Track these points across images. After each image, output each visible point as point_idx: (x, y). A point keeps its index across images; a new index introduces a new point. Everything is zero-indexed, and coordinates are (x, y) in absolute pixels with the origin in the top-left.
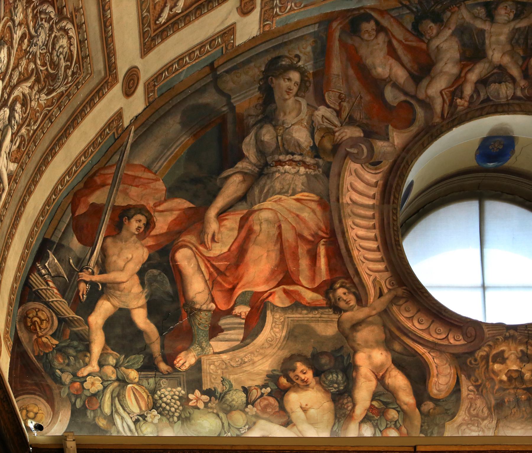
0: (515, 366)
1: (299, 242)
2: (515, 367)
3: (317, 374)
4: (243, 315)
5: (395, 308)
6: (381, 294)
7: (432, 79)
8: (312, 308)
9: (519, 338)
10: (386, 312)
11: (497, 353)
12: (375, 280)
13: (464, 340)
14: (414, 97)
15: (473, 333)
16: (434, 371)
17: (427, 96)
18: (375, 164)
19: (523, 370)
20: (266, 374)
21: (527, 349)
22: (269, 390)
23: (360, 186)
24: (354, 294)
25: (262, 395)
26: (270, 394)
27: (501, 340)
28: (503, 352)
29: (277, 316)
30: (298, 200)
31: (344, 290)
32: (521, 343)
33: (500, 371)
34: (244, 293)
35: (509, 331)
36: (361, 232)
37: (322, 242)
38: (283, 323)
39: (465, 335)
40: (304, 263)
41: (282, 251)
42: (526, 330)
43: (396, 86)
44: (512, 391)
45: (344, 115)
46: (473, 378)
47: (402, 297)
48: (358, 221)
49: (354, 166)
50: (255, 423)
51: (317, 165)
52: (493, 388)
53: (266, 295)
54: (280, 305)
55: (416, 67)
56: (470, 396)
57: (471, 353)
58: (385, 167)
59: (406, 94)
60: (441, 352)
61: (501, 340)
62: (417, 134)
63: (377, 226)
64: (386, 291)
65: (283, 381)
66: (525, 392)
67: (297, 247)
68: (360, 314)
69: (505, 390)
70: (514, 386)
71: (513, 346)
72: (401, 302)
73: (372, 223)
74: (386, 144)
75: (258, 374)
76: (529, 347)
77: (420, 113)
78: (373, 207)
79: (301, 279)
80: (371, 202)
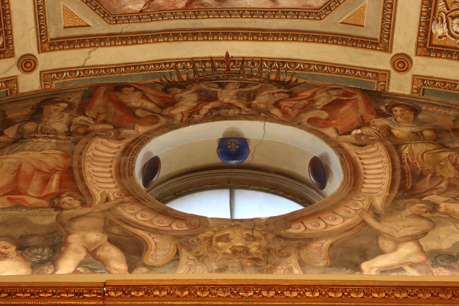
13: (187, 226)
19: (248, 246)
27: (226, 227)
28: (228, 235)
32: (246, 229)
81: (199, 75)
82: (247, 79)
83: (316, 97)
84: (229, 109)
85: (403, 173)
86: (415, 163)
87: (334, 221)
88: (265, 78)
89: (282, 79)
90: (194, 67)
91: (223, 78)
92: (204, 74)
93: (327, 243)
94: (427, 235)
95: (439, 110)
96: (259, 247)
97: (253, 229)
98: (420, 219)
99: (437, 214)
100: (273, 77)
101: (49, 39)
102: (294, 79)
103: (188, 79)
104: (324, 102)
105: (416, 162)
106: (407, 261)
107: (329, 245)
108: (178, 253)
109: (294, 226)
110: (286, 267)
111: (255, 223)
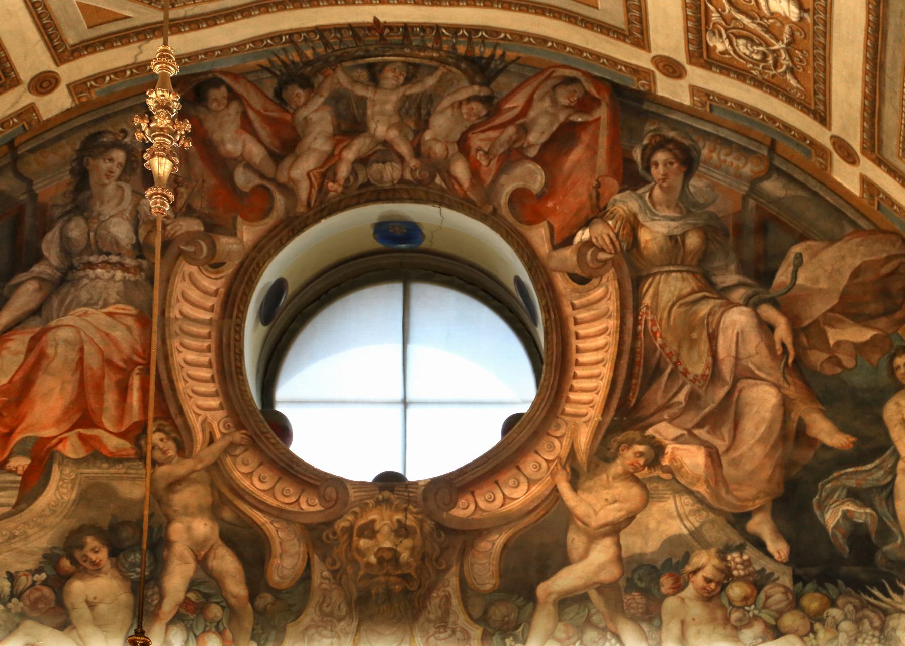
0: (387, 542)
1: (106, 369)
2: (387, 545)
3: (114, 553)
4: (20, 471)
5: (229, 460)
6: (212, 441)
7: (297, 157)
8: (116, 459)
9: (396, 503)
10: (216, 466)
11: (364, 524)
12: (204, 421)
13: (321, 505)
14: (273, 180)
15: (334, 496)
16: (277, 549)
17: (290, 179)
18: (217, 266)
19: (398, 549)
20: (41, 553)
21: (406, 518)
22: (44, 576)
23: (194, 294)
24: (175, 440)
25: (34, 583)
26: (44, 583)
27: (371, 505)
29: (67, 471)
30: (110, 314)
31: (162, 435)
32: (397, 510)
33: (368, 549)
34: (24, 440)
35: (382, 492)
36: (191, 357)
37: (137, 370)
38: (73, 481)
39: (322, 498)
40: (110, 398)
41: (82, 383)
42: (405, 491)
43: (249, 166)
44: (382, 579)
45: (181, 203)
46: (329, 560)
47: (241, 445)
48: (188, 341)
49: (188, 269)
50: (18, 625)
51: (139, 268)
52: (356, 573)
53: (54, 441)
54: (72, 456)
55: (277, 143)
56: (324, 586)
57: (329, 524)
58: (229, 270)
59: (262, 176)
60: (288, 521)
61: (371, 505)
62: (275, 227)
63: (213, 348)
64: (218, 435)
65: (66, 563)
66: (400, 579)
67: (103, 377)
68: (181, 468)
69: (373, 576)
70: (385, 571)
71: (387, 513)
72: (238, 452)
73: (205, 344)
74: (231, 240)
75: (32, 553)
76: (409, 516)
77: (280, 201)
78: (210, 322)
79: (104, 420)
80: (207, 316)
81: (333, 49)
82: (417, 52)
83: (532, 114)
84: (384, 162)
85: (632, 364)
86: (655, 334)
87: (515, 490)
88: (448, 52)
89: (477, 51)
90: (322, 37)
91: (376, 53)
92: (342, 47)
93: (499, 540)
94: (633, 523)
95: (729, 159)
96: (413, 550)
97: (406, 509)
98: (632, 484)
99: (658, 472)
100: (462, 49)
101: (68, 47)
102: (499, 52)
103: (318, 58)
104: (543, 133)
105: (656, 332)
106: (595, 579)
107: (502, 545)
108: (309, 565)
109: (462, 502)
110: (443, 594)
111: (411, 494)
